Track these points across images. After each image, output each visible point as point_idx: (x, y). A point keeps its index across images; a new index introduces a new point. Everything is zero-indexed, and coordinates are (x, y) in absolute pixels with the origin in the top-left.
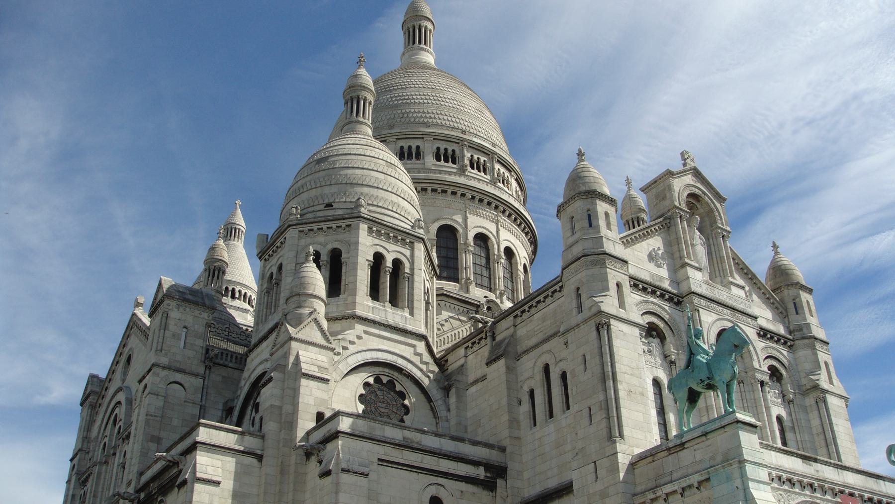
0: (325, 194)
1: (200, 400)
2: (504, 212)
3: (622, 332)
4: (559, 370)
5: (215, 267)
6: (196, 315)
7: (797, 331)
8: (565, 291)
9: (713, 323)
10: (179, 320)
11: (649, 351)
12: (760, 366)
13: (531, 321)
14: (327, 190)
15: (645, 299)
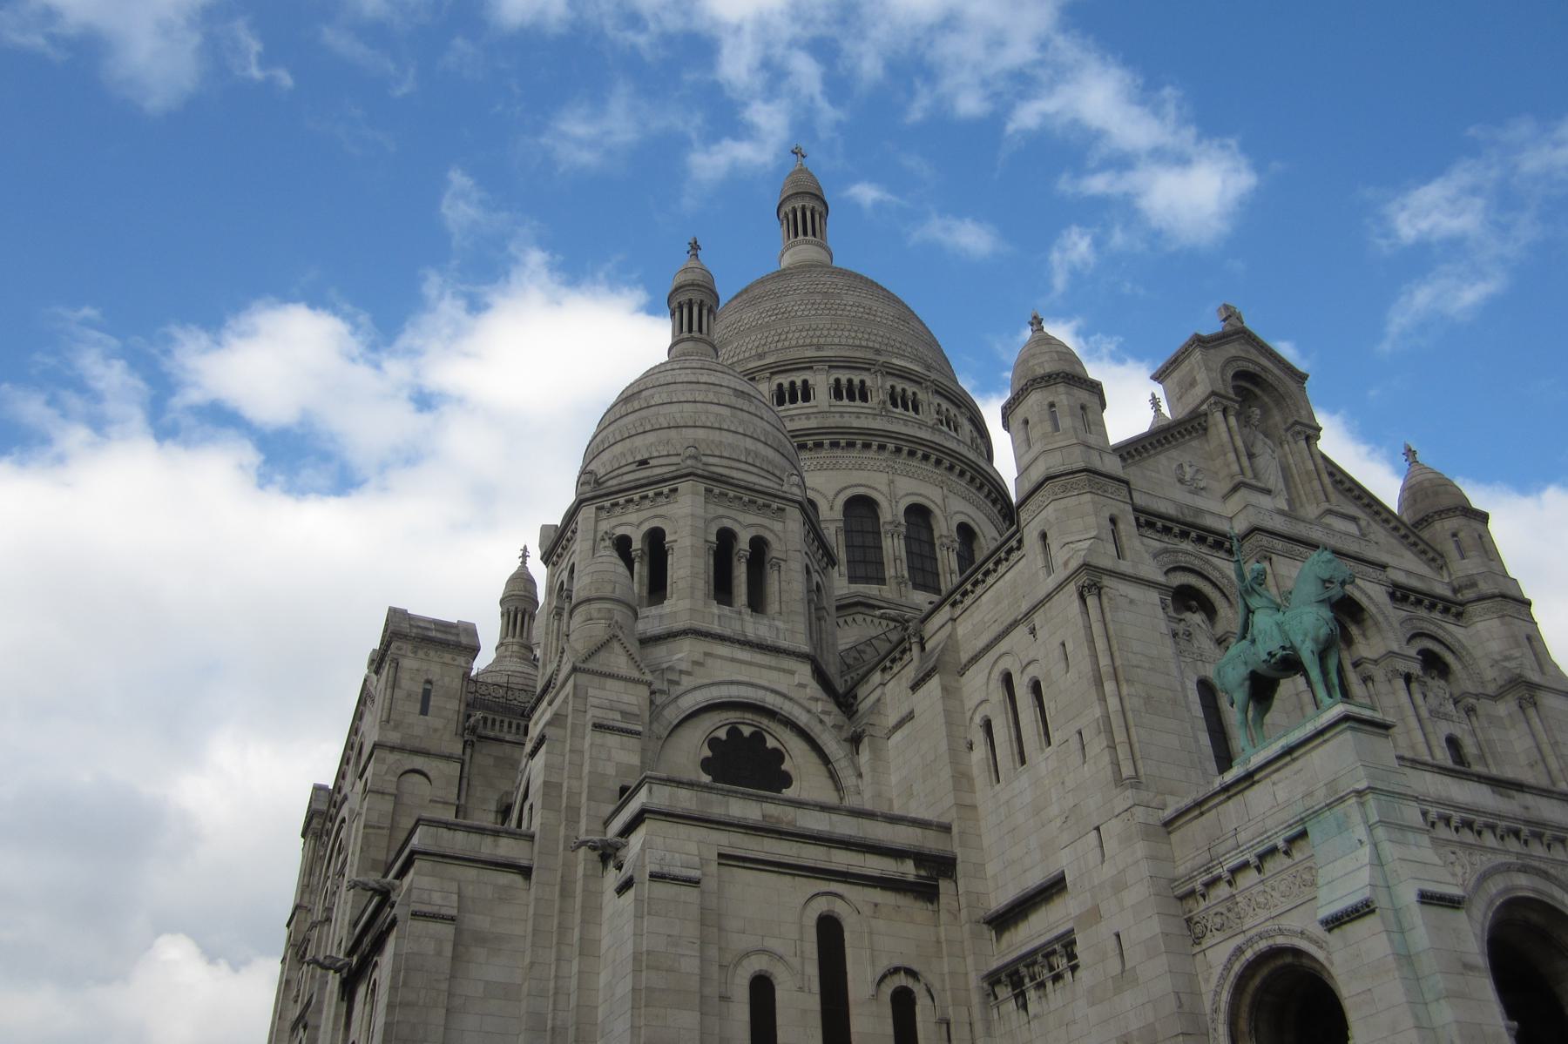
0: (636, 448)
1: (456, 797)
5: (516, 608)
7: (1467, 587)
8: (1026, 542)
11: (1187, 633)
15: (1169, 546)
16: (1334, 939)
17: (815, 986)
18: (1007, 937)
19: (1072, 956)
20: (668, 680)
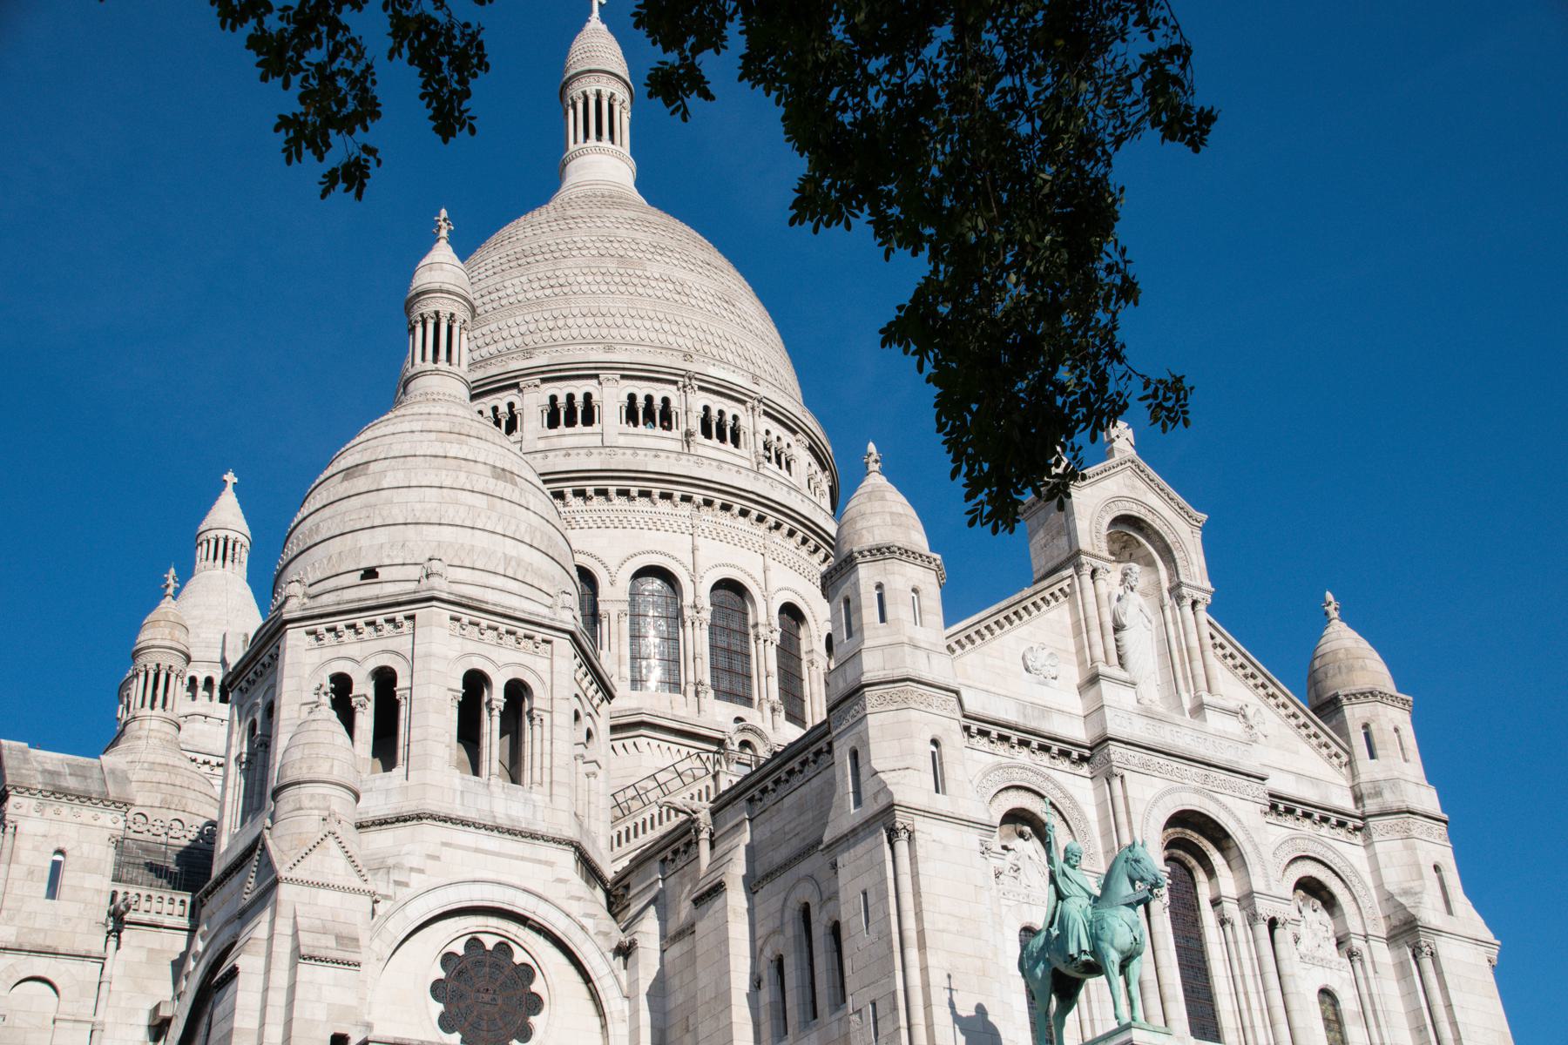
0: (360, 548)
3: (941, 843)
4: (826, 918)
5: (158, 665)
6: (85, 821)
9: (1156, 801)
10: (45, 836)
11: (1015, 868)
12: (1268, 886)
13: (779, 811)
20: (395, 881)
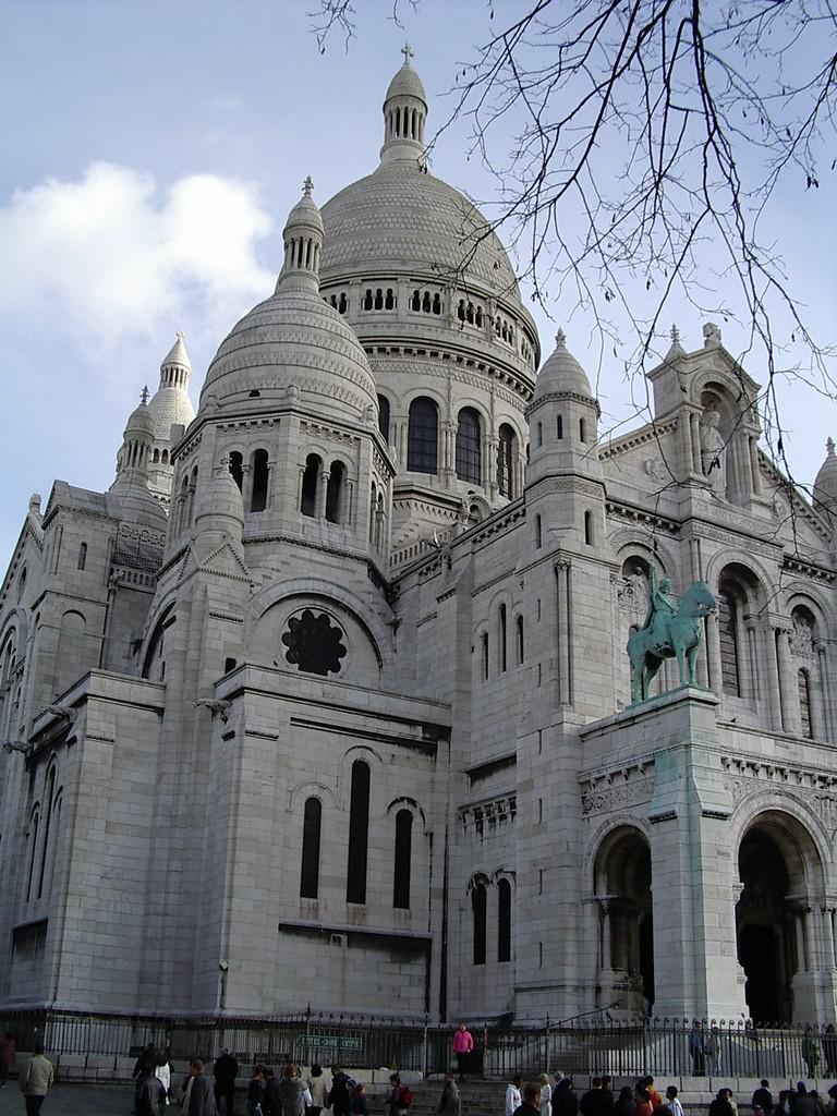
2: (502, 376)
12: (778, 611)
14: (253, 373)
16: (654, 828)
17: (348, 808)
18: (477, 783)
19: (513, 806)
